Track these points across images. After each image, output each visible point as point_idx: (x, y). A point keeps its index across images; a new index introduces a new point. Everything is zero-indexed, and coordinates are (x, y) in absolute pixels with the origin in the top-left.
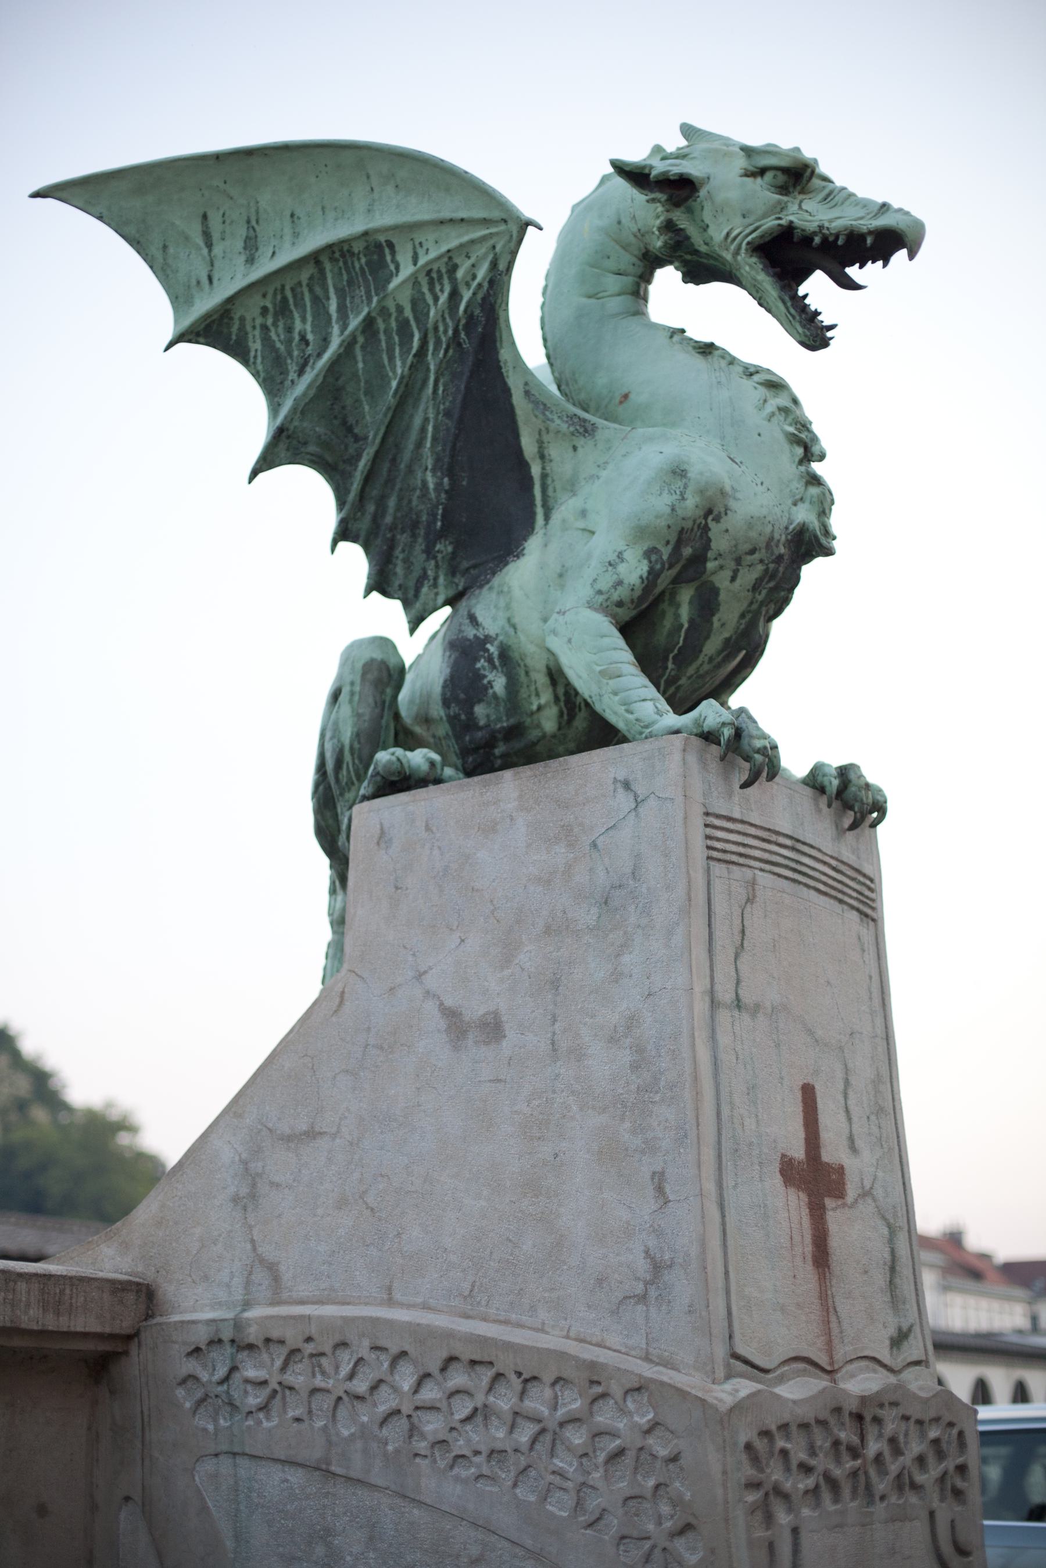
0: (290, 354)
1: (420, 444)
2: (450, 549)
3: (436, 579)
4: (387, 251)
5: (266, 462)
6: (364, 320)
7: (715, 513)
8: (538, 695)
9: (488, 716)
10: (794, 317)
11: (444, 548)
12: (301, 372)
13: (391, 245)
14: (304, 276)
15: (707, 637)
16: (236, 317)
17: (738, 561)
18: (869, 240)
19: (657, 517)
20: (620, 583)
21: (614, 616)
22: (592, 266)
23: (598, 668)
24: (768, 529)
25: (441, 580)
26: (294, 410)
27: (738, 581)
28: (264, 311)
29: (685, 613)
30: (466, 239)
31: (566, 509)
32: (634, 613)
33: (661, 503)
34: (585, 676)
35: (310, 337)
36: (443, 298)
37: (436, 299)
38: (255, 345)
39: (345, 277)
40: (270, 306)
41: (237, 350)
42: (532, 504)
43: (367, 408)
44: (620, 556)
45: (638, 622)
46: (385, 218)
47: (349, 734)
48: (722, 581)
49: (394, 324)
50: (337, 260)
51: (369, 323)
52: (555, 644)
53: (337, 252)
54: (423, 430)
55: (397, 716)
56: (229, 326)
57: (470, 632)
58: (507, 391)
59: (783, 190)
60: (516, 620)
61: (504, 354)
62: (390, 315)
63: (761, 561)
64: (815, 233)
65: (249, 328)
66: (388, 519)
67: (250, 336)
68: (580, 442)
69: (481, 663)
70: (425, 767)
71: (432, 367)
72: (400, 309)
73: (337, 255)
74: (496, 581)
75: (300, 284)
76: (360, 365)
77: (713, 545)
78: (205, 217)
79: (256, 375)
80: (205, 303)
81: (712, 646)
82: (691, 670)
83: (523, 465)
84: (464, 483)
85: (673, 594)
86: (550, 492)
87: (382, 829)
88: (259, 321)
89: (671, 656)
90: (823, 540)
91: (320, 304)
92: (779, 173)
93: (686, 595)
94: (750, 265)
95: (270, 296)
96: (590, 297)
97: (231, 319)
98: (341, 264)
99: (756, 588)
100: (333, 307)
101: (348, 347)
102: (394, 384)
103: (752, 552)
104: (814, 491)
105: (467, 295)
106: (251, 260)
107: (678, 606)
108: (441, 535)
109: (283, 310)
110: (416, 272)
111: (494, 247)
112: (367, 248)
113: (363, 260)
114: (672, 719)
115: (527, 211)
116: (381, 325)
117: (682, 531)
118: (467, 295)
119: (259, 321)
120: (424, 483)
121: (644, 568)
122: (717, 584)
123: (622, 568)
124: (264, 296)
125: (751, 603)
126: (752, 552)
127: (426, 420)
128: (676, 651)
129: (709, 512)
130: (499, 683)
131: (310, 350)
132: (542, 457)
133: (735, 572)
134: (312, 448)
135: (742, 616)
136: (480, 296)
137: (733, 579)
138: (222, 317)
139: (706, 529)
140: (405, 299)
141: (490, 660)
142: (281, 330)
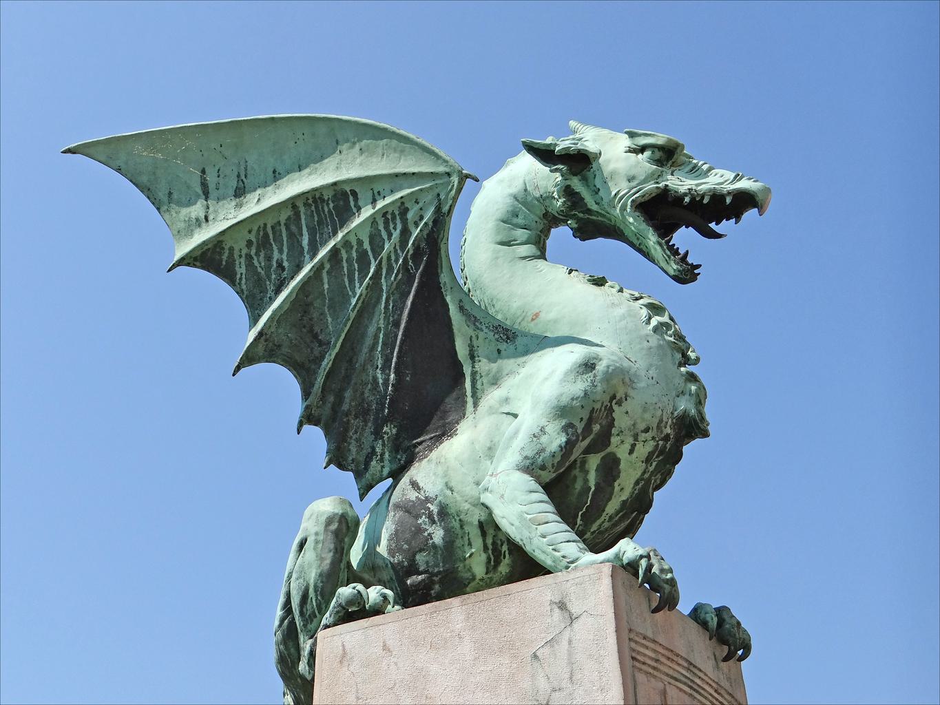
0: (269, 278)
1: (373, 348)
2: (394, 431)
3: (382, 455)
4: (351, 198)
6: (331, 250)
7: (618, 398)
8: (470, 544)
9: (427, 563)
10: (669, 257)
11: (389, 430)
13: (354, 193)
14: (283, 218)
15: (610, 499)
16: (227, 248)
17: (636, 437)
18: (728, 200)
19: (573, 399)
21: (538, 480)
22: (504, 222)
23: (529, 517)
25: (387, 455)
27: (635, 455)
28: (249, 243)
32: (554, 475)
34: (517, 523)
35: (286, 264)
36: (396, 235)
37: (390, 235)
38: (241, 270)
39: (316, 219)
40: (254, 240)
41: (227, 274)
42: (465, 395)
43: (330, 320)
44: (542, 430)
45: (559, 482)
47: (313, 575)
48: (622, 453)
49: (354, 255)
50: (310, 205)
52: (487, 498)
53: (313, 198)
54: (376, 337)
55: (349, 564)
56: (220, 254)
59: (659, 162)
60: (452, 484)
61: (444, 278)
62: (352, 247)
63: (653, 438)
64: (685, 194)
65: (236, 256)
66: (345, 407)
67: (237, 262)
69: (423, 520)
71: (384, 288)
72: (360, 243)
73: (310, 201)
75: (279, 223)
76: (326, 286)
77: (616, 423)
78: (203, 172)
81: (612, 507)
82: (594, 527)
83: (458, 366)
84: (408, 379)
85: (584, 462)
86: (479, 386)
87: (344, 649)
88: (244, 252)
89: (580, 513)
91: (294, 238)
92: (656, 150)
93: (594, 461)
94: (633, 222)
95: (254, 232)
96: (502, 243)
97: (223, 248)
98: (313, 208)
99: (648, 460)
100: (305, 242)
101: (318, 270)
102: (354, 301)
103: (647, 430)
107: (587, 472)
108: (386, 421)
109: (264, 243)
110: (374, 213)
111: (439, 195)
112: (335, 196)
114: (590, 557)
116: (344, 255)
120: (375, 379)
122: (619, 455)
123: (544, 439)
124: (250, 232)
125: (644, 472)
126: (647, 430)
127: (379, 329)
128: (584, 510)
129: (614, 397)
131: (285, 274)
133: (633, 446)
134: (285, 350)
135: (637, 483)
136: (425, 233)
137: (631, 452)
138: (215, 246)
139: (611, 410)
141: (430, 516)
142: (262, 258)
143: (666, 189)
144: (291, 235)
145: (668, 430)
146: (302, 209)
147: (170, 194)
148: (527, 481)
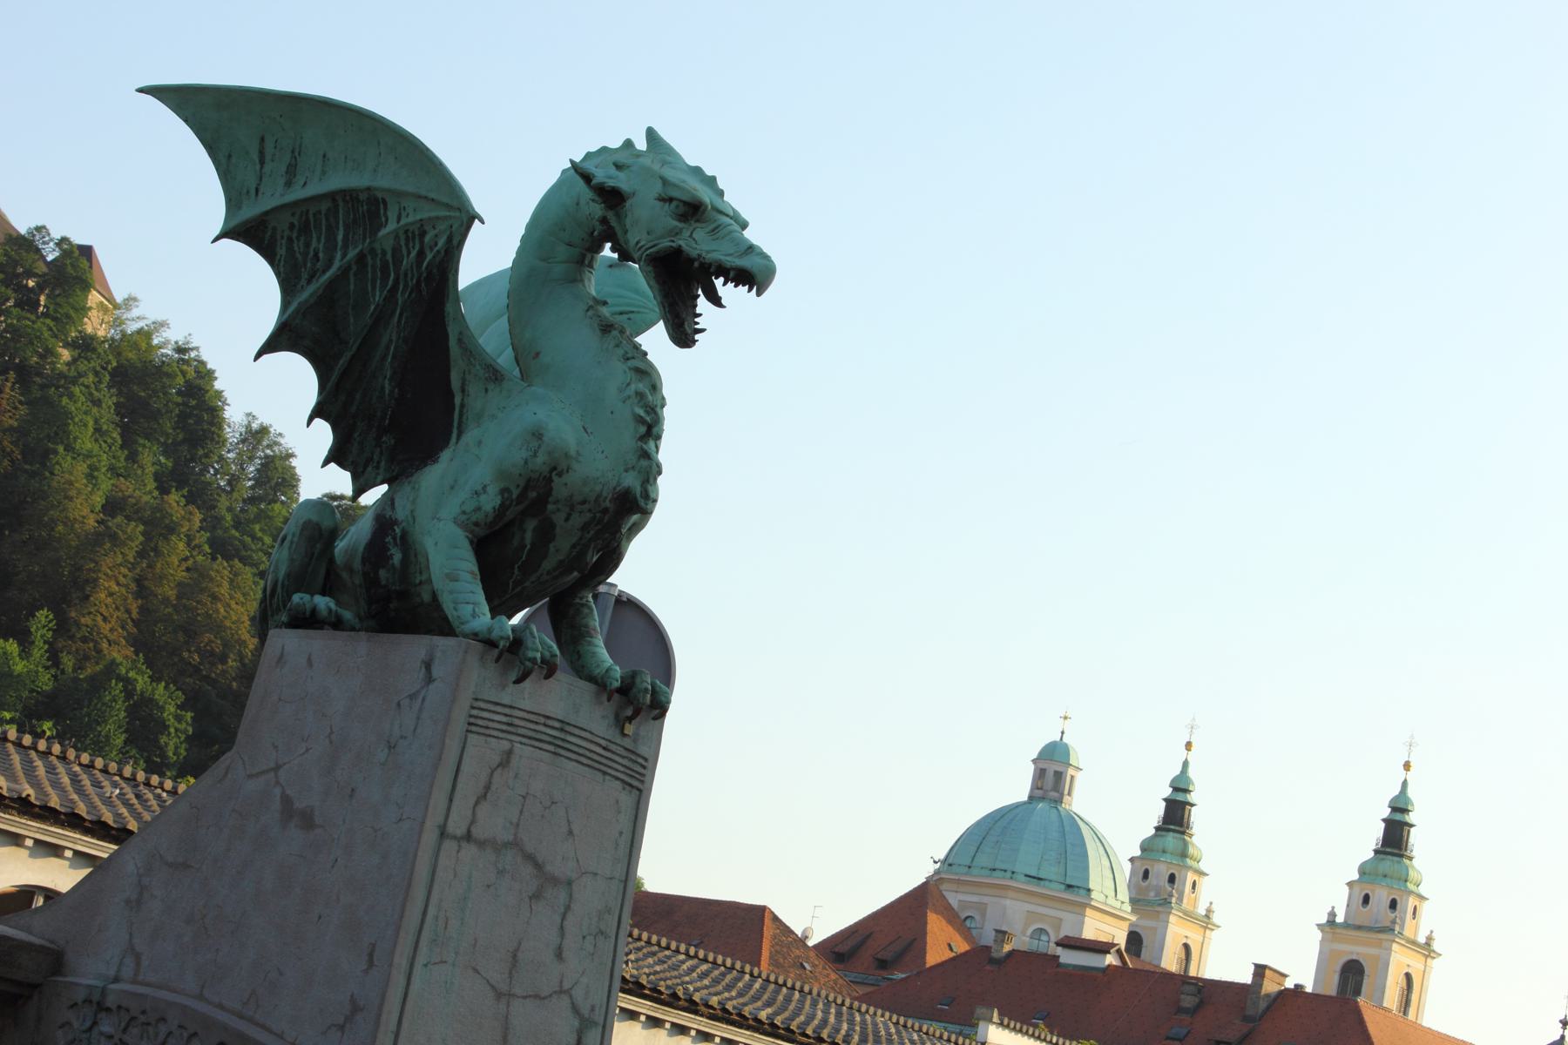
1: (384, 358)
5: (270, 346)
11: (389, 440)
12: (309, 281)
14: (324, 206)
17: (572, 508)
20: (478, 509)
21: (472, 532)
24: (598, 488)
26: (297, 311)
28: (292, 226)
29: (529, 536)
30: (434, 214)
31: (470, 437)
33: (519, 455)
36: (413, 254)
38: (281, 251)
46: (383, 181)
48: (559, 519)
51: (361, 258)
53: (348, 196)
54: (388, 348)
55: (332, 560)
57: (388, 513)
58: (445, 337)
61: (449, 308)
66: (353, 409)
68: (491, 386)
69: (389, 539)
70: (324, 613)
72: (384, 253)
74: (414, 479)
78: (263, 139)
79: (278, 274)
80: (250, 211)
81: (548, 565)
82: (533, 578)
83: (451, 395)
88: (287, 233)
90: (642, 502)
91: (332, 231)
93: (531, 525)
99: (585, 528)
101: (345, 271)
103: (584, 502)
104: (644, 463)
105: (429, 256)
106: (289, 184)
107: (525, 531)
109: (305, 229)
113: (364, 208)
115: (478, 206)
116: (370, 261)
117: (529, 480)
118: (429, 256)
119: (287, 233)
120: (383, 388)
121: (498, 501)
123: (483, 498)
129: (555, 468)
130: (397, 557)
131: (319, 265)
132: (463, 391)
135: (574, 546)
137: (567, 520)
139: (550, 480)
140: (388, 245)
141: (394, 538)
143: (678, 251)
144: (329, 227)
145: (607, 504)
146: (341, 204)
147: (230, 156)
148: (461, 538)
